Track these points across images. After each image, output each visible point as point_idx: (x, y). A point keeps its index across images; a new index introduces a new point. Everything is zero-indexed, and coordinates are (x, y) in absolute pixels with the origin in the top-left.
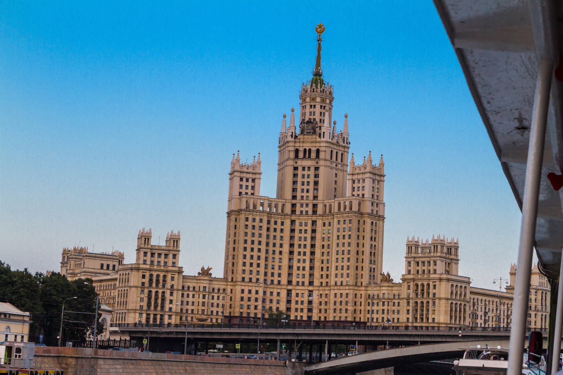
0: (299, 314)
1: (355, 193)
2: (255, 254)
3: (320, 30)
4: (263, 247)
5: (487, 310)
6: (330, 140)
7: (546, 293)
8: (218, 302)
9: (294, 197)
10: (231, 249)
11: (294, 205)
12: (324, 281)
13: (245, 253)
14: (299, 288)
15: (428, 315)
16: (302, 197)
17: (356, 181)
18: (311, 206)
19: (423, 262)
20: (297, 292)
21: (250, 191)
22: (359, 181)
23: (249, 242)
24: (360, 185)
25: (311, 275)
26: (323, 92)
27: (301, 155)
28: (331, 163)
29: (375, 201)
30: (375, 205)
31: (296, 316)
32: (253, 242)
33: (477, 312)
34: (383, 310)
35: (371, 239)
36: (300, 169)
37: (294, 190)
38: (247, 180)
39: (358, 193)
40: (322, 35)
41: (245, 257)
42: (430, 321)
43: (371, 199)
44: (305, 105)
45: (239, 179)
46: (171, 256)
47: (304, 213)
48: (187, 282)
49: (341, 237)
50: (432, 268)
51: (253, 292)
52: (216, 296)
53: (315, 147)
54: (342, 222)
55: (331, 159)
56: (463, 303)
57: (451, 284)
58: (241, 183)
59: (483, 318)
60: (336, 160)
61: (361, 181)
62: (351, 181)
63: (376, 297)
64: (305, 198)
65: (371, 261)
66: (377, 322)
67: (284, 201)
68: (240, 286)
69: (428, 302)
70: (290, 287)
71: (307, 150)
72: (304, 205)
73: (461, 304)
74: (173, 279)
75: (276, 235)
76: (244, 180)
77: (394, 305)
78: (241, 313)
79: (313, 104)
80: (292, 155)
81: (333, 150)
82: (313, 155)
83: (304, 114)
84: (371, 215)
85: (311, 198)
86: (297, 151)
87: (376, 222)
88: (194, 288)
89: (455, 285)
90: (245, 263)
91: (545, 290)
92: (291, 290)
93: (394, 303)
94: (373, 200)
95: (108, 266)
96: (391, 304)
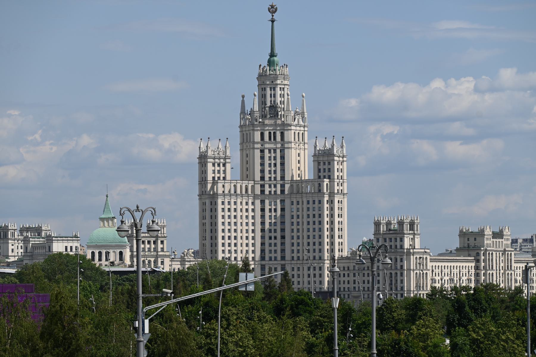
1: (322, 174)
3: (273, 10)
7: (492, 254)
9: (263, 178)
10: (208, 231)
11: (262, 186)
12: (295, 255)
14: (271, 262)
15: (396, 284)
16: (270, 178)
17: (322, 164)
18: (279, 186)
19: (391, 240)
21: (222, 175)
22: (324, 164)
24: (326, 167)
25: (283, 251)
27: (266, 138)
28: (295, 144)
34: (355, 281)
35: (339, 217)
36: (266, 151)
37: (262, 171)
38: (219, 165)
39: (325, 174)
40: (275, 15)
42: (399, 289)
44: (265, 87)
45: (211, 164)
46: (159, 242)
47: (273, 193)
49: (311, 216)
50: (398, 244)
54: (311, 202)
57: (415, 257)
59: (440, 281)
60: (298, 140)
61: (327, 163)
62: (316, 163)
63: (346, 269)
64: (273, 179)
65: (339, 236)
66: (349, 290)
67: (253, 182)
69: (396, 273)
70: (263, 263)
72: (273, 186)
77: (364, 276)
82: (279, 138)
83: (263, 97)
85: (279, 178)
86: (262, 135)
87: (341, 200)
89: (418, 257)
91: (491, 250)
92: (264, 265)
93: (364, 274)
94: (338, 180)
95: (71, 247)
96: (361, 275)
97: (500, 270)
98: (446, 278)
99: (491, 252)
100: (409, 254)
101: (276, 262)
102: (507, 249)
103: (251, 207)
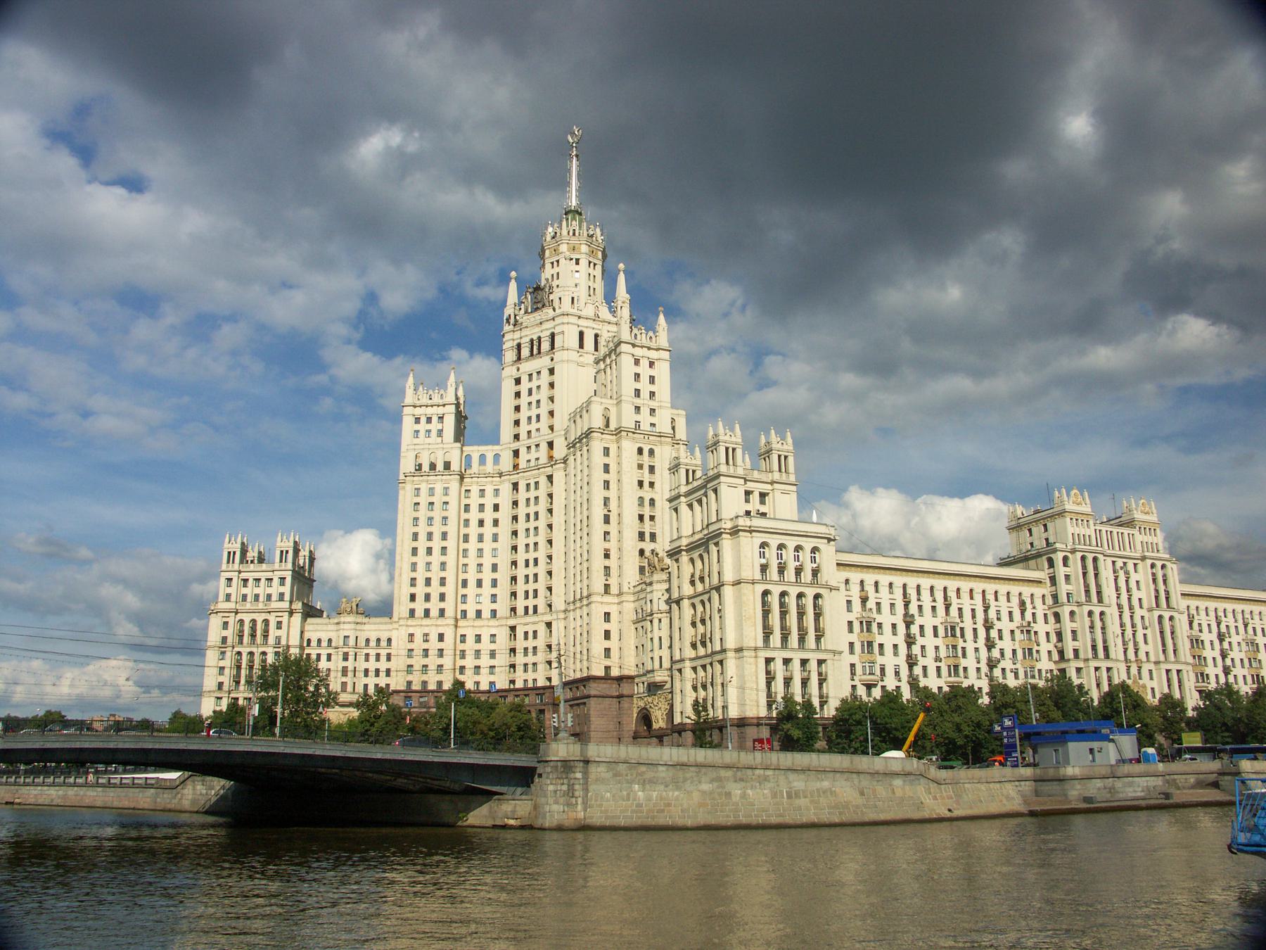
0: (530, 676)
2: (436, 558)
4: (451, 544)
5: (913, 609)
6: (575, 311)
7: (1095, 559)
8: (378, 665)
9: (517, 437)
11: (516, 453)
13: (414, 559)
18: (544, 446)
20: (526, 628)
23: (422, 537)
26: (574, 234)
27: (525, 352)
29: (646, 402)
30: (645, 411)
31: (526, 681)
32: (430, 536)
33: (875, 615)
36: (525, 379)
38: (429, 420)
41: (414, 567)
43: (631, 399)
48: (316, 631)
51: (434, 637)
52: (373, 652)
53: (547, 329)
55: (581, 346)
56: (810, 592)
58: (417, 427)
68: (404, 628)
70: (512, 622)
71: (535, 337)
72: (533, 448)
73: (800, 596)
74: (279, 625)
75: (478, 514)
76: (423, 420)
78: (409, 683)
79: (554, 259)
80: (510, 356)
81: (584, 329)
82: (546, 346)
84: (634, 433)
88: (330, 641)
90: (415, 579)
97: (1131, 607)
98: (928, 621)
99: (1090, 557)
100: (735, 532)
101: (535, 619)
102: (1146, 554)
103: (489, 501)
